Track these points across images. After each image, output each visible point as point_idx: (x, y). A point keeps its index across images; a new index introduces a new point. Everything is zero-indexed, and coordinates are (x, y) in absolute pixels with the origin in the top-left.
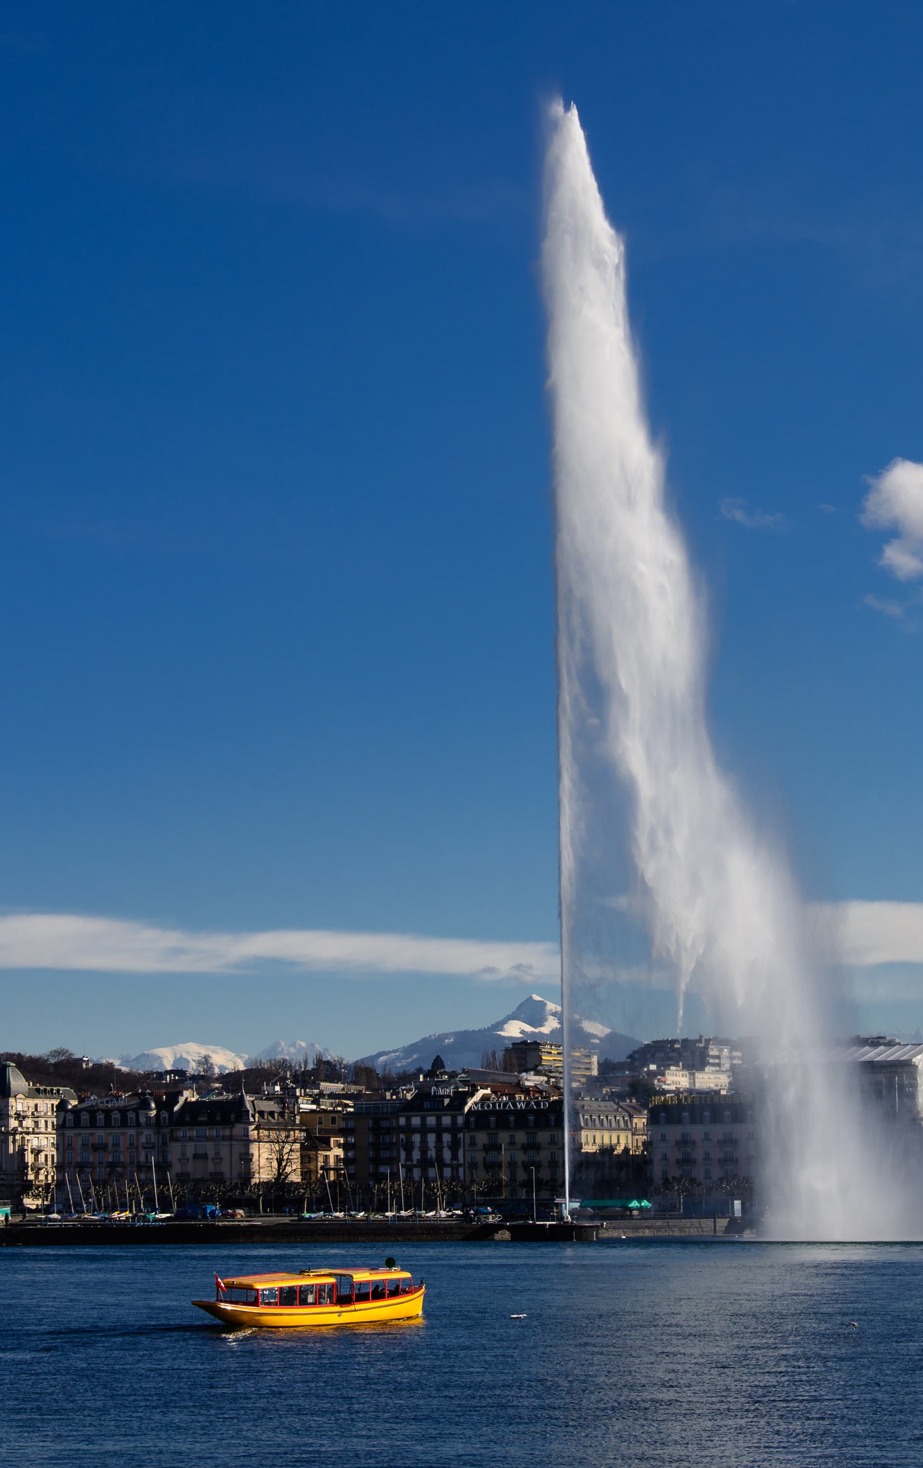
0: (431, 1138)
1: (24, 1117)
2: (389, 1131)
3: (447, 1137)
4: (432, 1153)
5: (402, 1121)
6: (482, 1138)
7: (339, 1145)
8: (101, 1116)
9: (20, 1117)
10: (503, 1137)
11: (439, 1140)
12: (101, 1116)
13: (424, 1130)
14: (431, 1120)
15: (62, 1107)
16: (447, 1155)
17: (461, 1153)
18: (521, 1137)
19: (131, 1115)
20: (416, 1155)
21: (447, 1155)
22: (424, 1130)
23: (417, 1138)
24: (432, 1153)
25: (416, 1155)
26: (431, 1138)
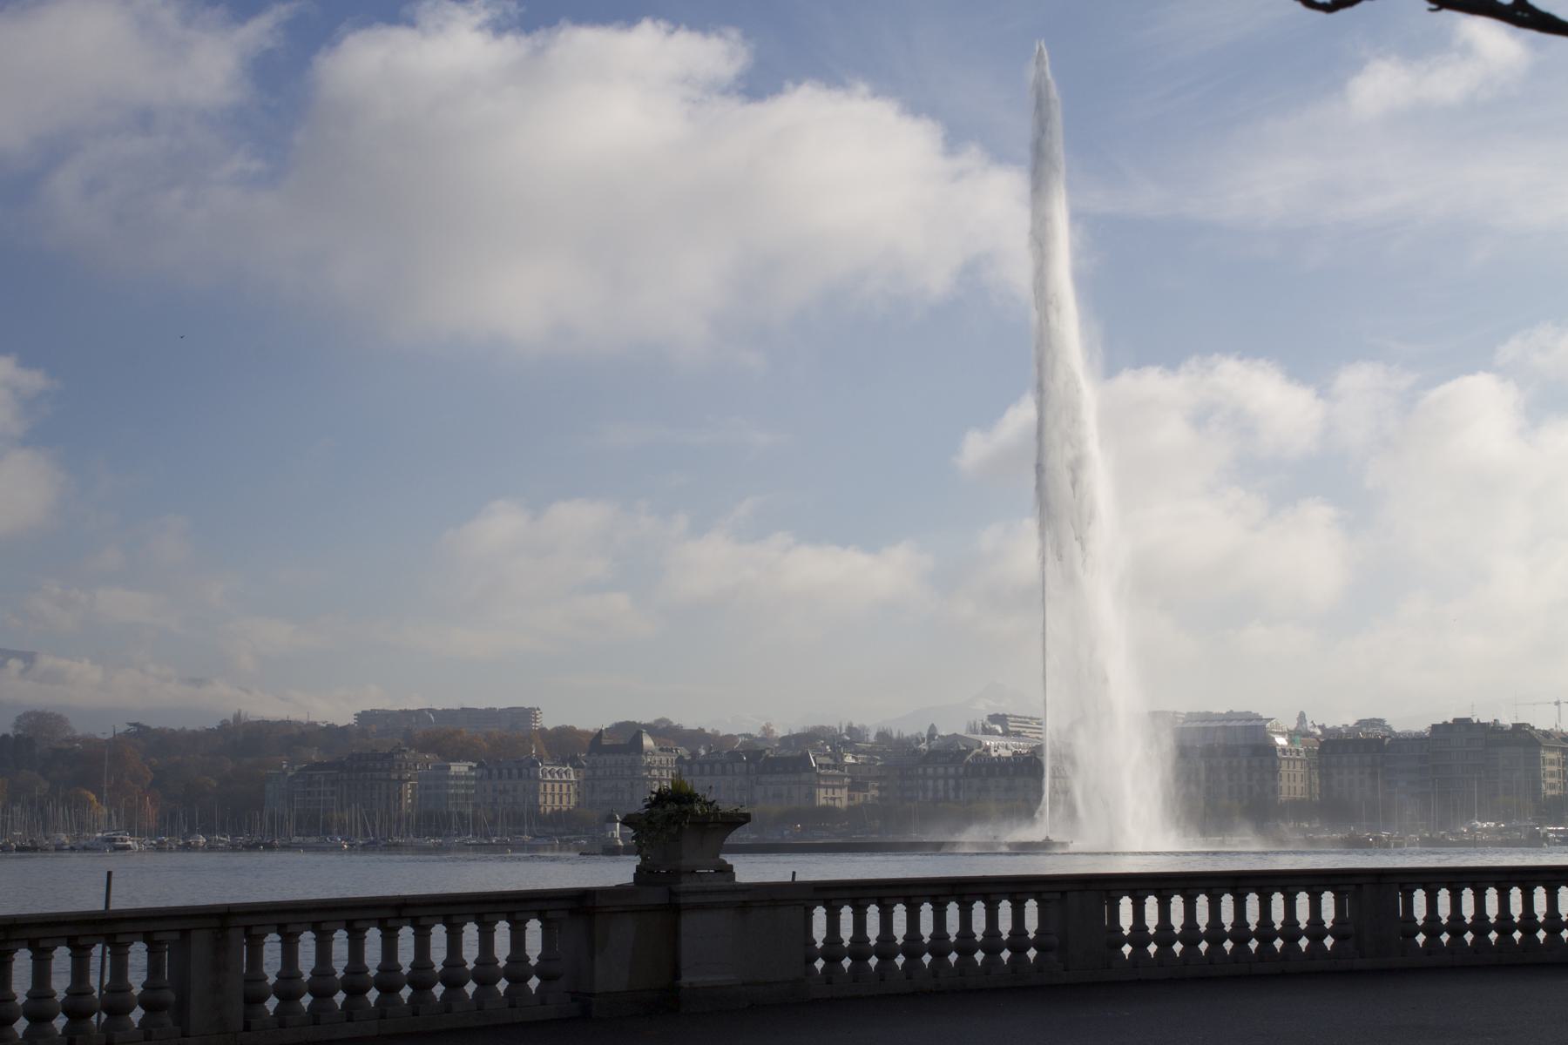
1: (654, 768)
5: (920, 771)
7: (878, 788)
8: (707, 768)
9: (649, 768)
11: (946, 784)
12: (707, 768)
15: (680, 759)
16: (952, 795)
17: (961, 793)
19: (729, 767)
21: (952, 795)
23: (930, 783)
24: (941, 794)
25: (930, 795)
26: (941, 783)
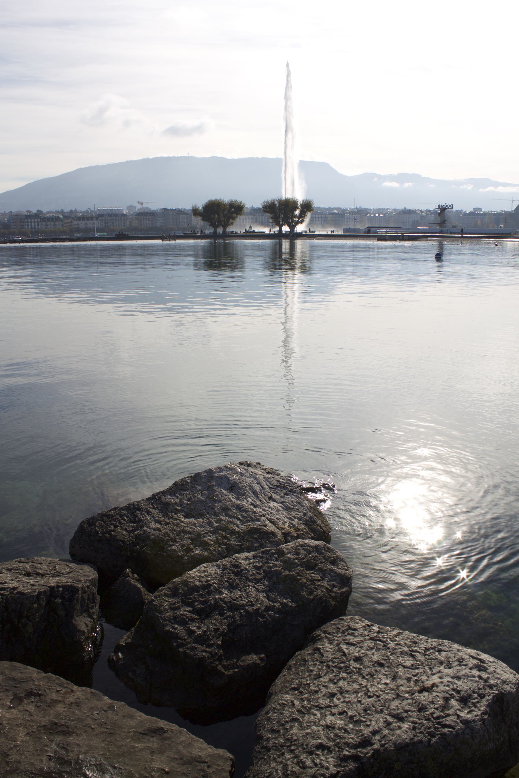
0: (33, 224)
2: (23, 222)
3: (36, 224)
4: (33, 227)
6: (44, 223)
10: (49, 223)
13: (31, 222)
14: (33, 220)
16: (37, 227)
18: (52, 223)
20: (30, 227)
22: (31, 222)
23: (30, 224)
24: (33, 227)
25: (30, 227)
26: (33, 224)
